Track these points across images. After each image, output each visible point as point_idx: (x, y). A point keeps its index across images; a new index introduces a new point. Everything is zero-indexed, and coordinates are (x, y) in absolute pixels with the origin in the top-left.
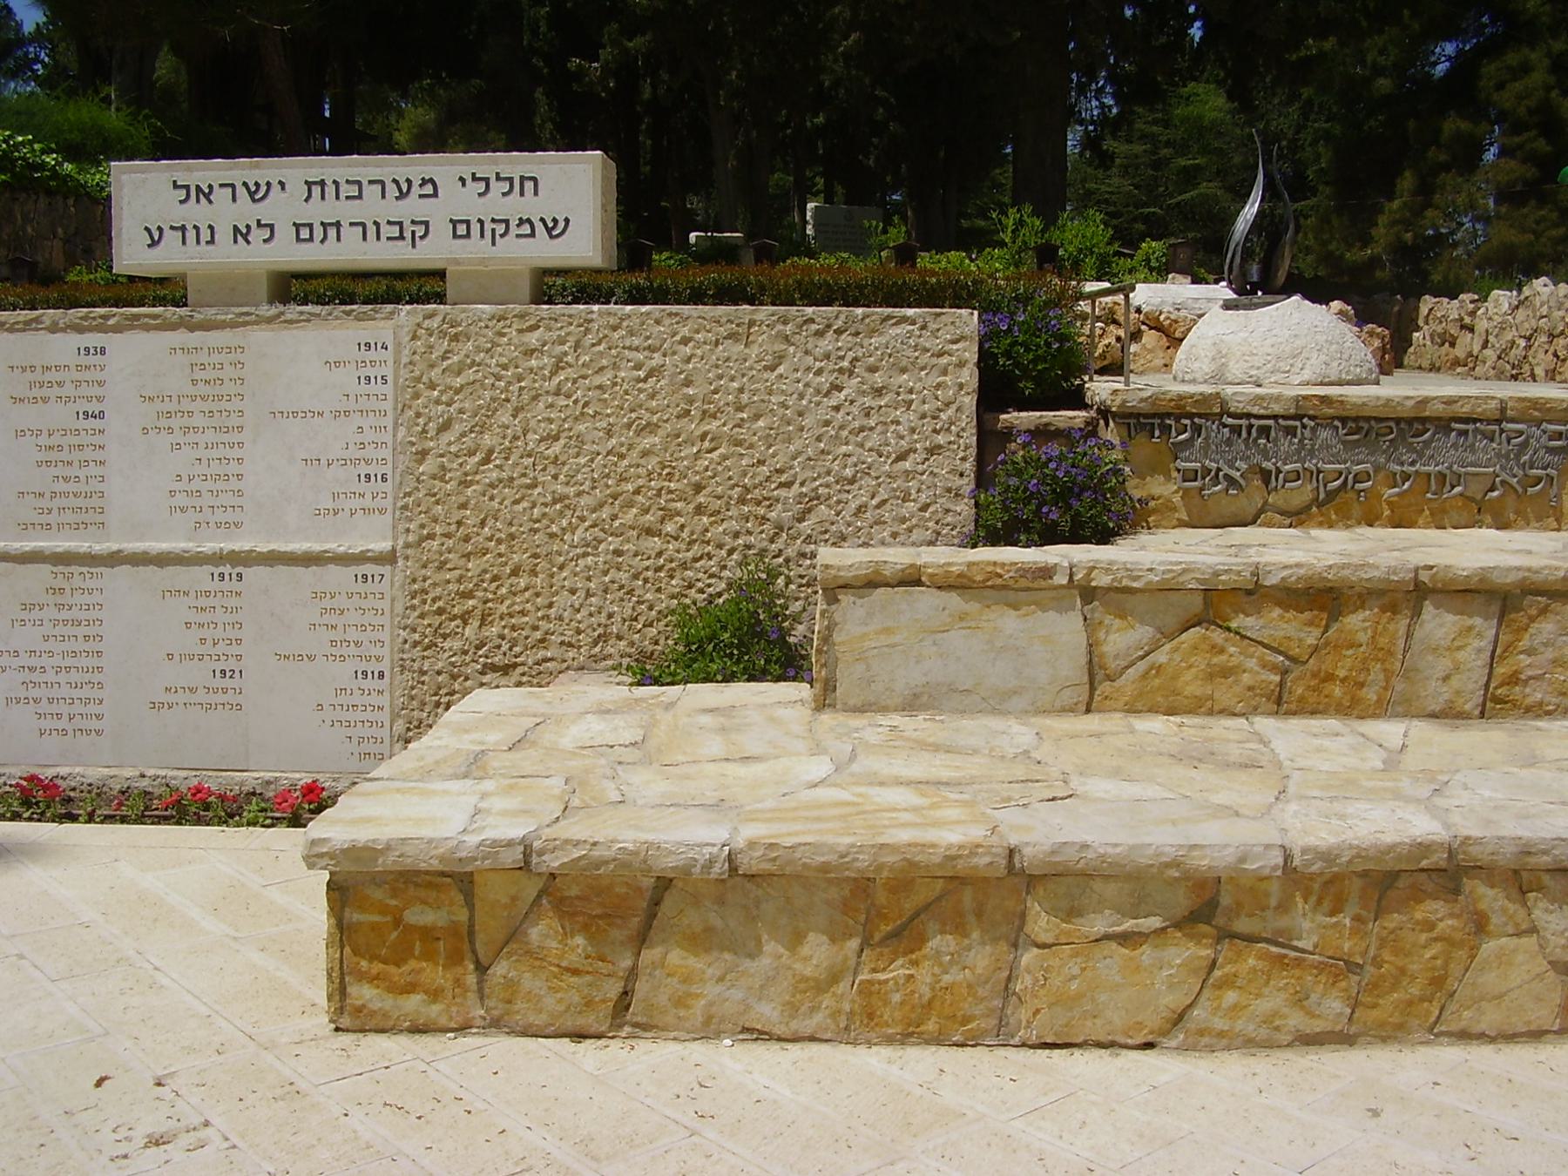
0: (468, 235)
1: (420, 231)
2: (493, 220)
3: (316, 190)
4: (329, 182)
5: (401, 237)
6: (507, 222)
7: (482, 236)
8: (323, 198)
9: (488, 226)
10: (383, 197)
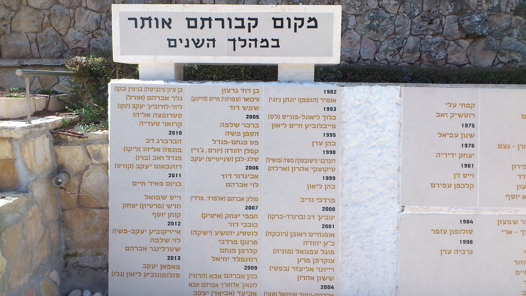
0: (282, 27)
1: (253, 23)
5: (243, 27)
6: (302, 20)
7: (289, 27)
9: (293, 22)
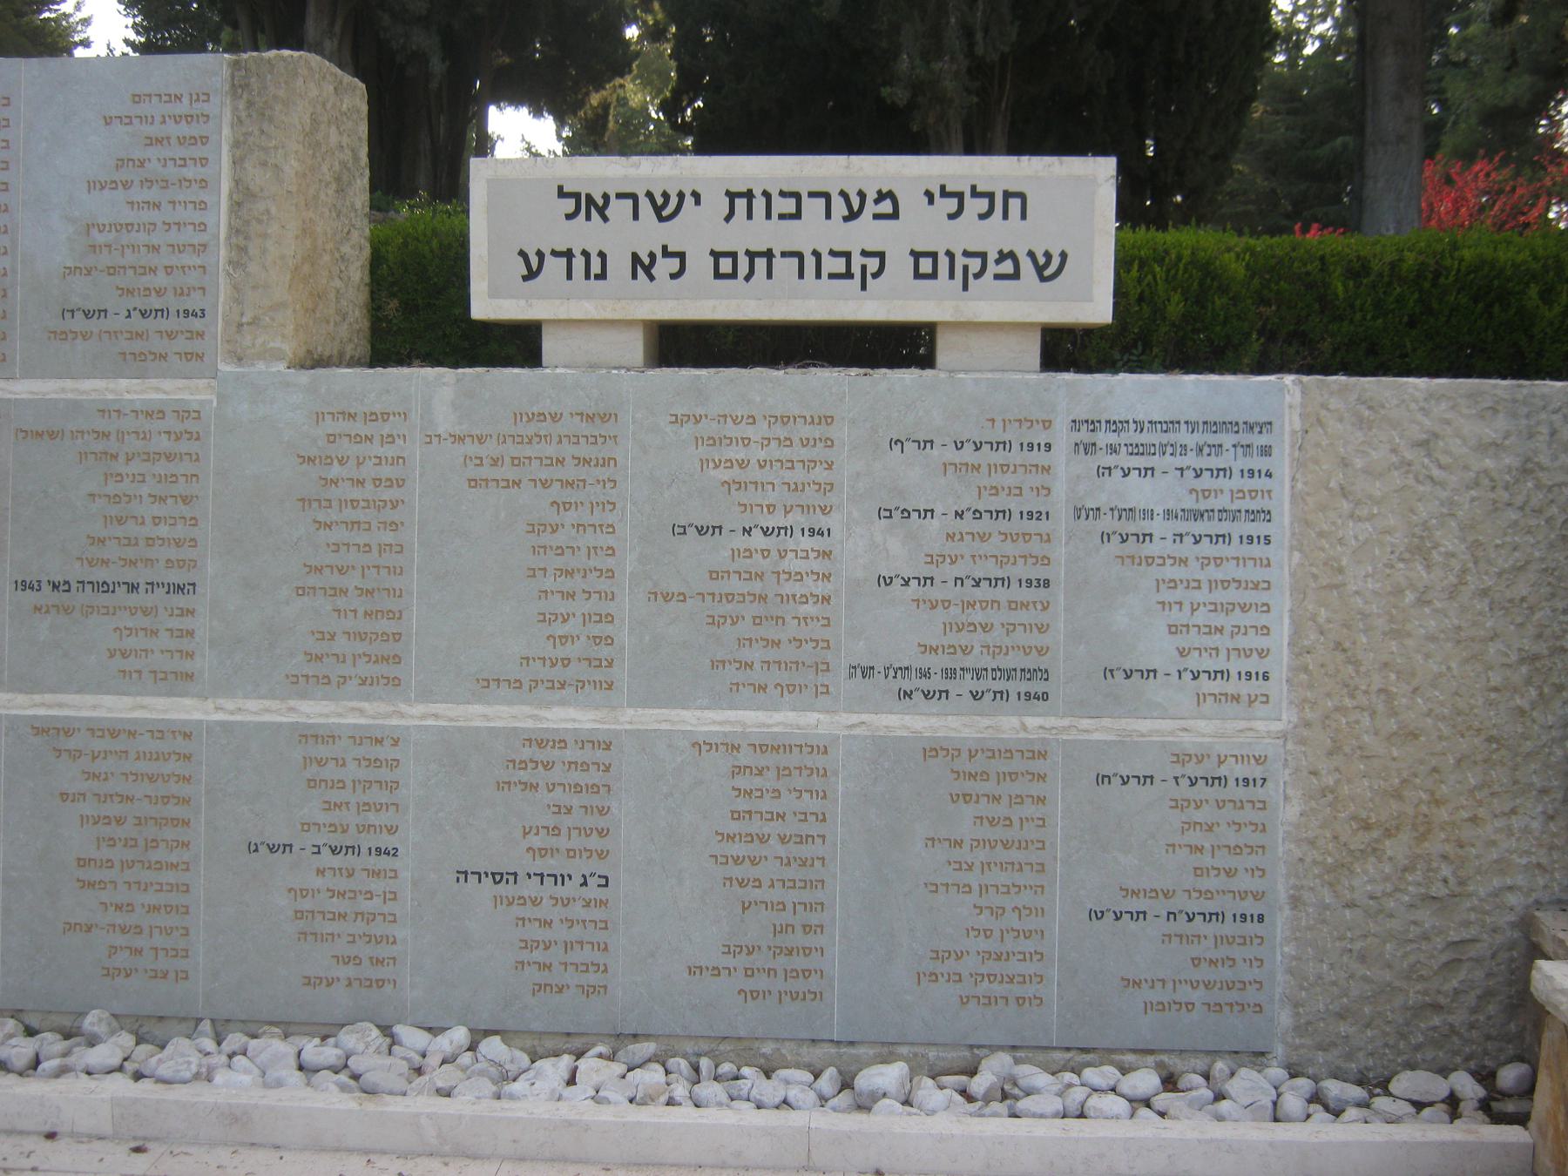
0: (934, 275)
1: (873, 265)
2: (966, 254)
3: (741, 203)
4: (757, 192)
5: (848, 275)
6: (983, 256)
7: (952, 276)
8: (750, 216)
9: (960, 261)
10: (828, 216)
